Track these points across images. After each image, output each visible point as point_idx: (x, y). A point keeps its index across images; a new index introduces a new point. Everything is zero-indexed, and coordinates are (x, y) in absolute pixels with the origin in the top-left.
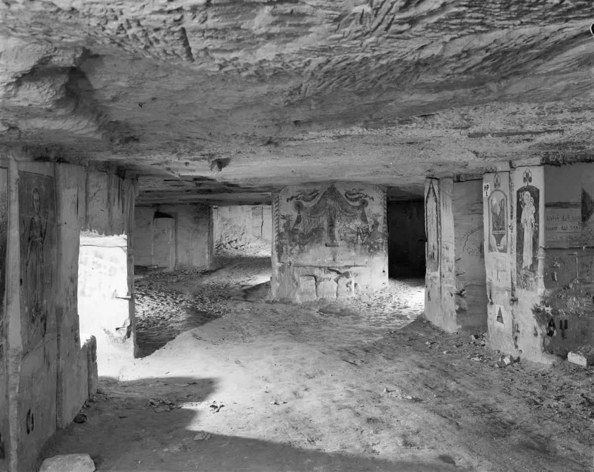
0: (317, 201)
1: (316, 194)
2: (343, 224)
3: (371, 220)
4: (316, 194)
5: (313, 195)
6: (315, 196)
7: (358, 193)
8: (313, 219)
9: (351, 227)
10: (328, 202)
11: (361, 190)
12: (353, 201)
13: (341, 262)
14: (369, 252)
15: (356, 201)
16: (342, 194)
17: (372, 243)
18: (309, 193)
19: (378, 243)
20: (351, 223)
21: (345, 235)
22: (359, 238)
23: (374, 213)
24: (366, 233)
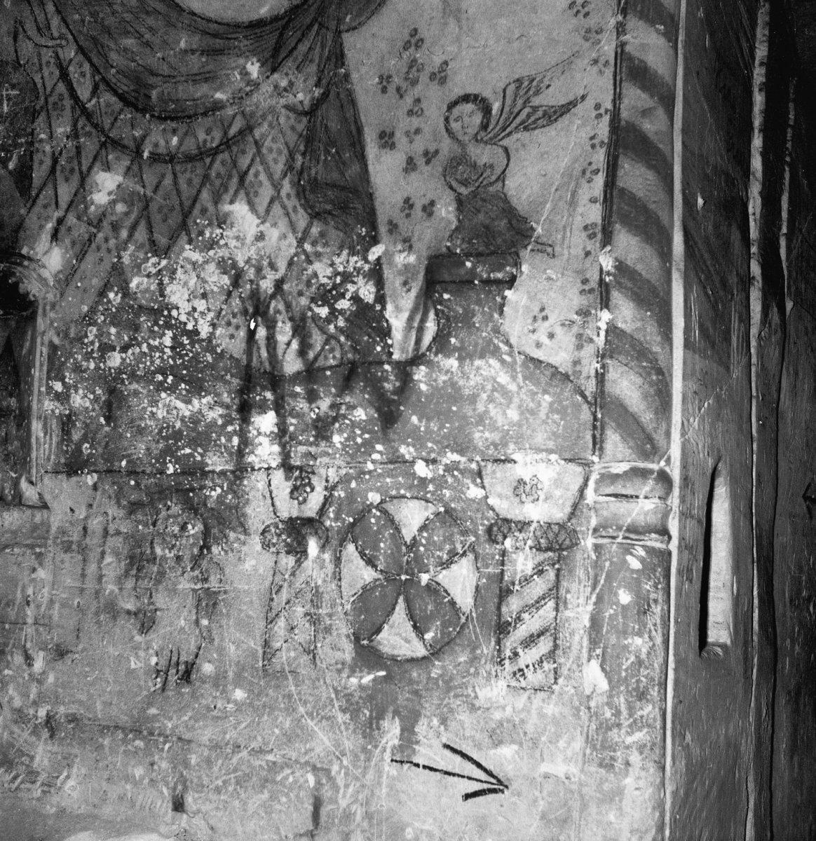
2: (93, 272)
3: (426, 185)
9: (177, 294)
13: (42, 754)
14: (368, 655)
17: (412, 516)
19: (500, 528)
21: (113, 403)
22: (266, 452)
23: (461, 83)
24: (349, 376)
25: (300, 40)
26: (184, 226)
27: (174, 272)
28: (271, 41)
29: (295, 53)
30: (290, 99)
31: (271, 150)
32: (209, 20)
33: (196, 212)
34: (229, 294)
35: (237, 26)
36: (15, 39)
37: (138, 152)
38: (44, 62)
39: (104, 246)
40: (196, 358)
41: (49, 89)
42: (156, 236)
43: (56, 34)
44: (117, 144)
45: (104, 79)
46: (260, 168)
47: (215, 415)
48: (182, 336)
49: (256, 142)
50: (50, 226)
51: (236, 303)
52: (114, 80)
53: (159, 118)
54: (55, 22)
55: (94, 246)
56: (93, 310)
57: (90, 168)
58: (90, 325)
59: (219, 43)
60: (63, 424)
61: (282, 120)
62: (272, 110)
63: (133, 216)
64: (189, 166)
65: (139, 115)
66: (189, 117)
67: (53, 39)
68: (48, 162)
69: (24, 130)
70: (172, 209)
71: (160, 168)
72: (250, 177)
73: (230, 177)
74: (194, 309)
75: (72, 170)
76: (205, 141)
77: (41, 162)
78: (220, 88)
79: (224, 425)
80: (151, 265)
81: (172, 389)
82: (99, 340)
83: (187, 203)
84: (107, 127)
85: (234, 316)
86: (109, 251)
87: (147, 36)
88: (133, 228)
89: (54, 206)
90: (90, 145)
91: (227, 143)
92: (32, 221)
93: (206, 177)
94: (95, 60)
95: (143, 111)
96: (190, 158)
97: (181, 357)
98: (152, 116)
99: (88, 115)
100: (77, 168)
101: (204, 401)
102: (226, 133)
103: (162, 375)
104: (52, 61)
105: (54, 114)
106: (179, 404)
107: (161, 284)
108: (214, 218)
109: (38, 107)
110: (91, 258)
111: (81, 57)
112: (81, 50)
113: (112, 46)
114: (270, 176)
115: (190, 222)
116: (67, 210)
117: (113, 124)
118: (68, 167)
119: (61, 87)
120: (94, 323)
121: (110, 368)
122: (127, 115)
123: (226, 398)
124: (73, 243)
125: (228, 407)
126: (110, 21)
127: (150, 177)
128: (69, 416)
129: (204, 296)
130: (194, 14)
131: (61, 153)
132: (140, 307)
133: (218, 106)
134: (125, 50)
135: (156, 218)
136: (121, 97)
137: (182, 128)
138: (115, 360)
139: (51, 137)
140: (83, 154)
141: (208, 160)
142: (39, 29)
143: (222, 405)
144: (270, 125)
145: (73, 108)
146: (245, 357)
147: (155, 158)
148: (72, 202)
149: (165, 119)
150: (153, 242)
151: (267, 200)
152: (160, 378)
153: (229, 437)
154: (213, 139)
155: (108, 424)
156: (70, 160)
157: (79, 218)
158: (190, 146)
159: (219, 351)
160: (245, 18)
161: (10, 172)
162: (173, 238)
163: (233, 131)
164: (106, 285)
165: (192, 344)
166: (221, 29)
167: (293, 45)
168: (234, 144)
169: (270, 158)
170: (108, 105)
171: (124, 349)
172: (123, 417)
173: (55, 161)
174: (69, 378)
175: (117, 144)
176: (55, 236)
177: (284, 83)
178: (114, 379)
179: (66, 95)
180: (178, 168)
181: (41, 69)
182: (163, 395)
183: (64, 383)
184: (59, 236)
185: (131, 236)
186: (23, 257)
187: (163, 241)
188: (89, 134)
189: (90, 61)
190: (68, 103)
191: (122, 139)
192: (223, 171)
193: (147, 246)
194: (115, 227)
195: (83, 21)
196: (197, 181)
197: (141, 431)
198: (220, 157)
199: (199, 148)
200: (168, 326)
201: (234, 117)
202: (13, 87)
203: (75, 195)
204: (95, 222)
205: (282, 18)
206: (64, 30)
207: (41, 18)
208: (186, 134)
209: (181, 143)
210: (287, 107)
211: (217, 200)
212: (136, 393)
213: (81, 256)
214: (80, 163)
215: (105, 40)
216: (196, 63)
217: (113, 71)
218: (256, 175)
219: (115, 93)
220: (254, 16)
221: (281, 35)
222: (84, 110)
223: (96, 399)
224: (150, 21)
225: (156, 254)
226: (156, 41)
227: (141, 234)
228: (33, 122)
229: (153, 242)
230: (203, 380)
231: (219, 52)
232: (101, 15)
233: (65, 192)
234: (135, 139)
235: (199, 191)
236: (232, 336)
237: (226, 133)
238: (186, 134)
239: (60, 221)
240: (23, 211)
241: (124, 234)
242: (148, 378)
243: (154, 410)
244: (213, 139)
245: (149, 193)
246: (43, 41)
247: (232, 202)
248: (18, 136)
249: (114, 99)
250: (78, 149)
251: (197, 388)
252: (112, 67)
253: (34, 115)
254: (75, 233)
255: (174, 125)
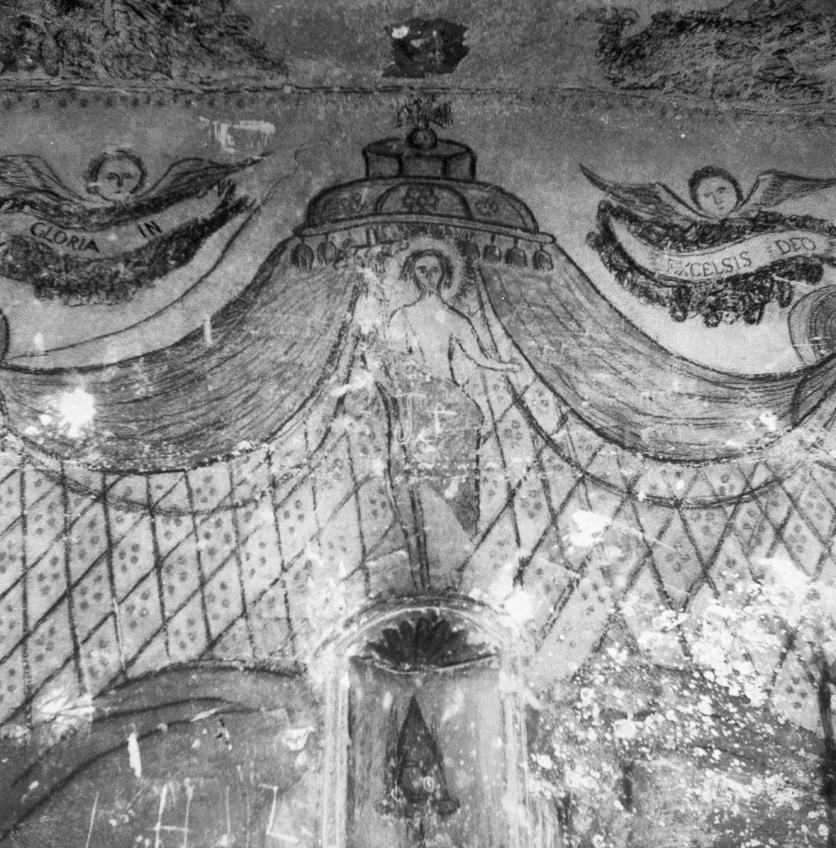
0: (216, 296)
1: (202, 208)
4: (202, 208)
5: (170, 220)
6: (191, 237)
7: (764, 223)
8: (130, 527)
9: (708, 653)
10: (367, 316)
11: (812, 185)
12: (713, 314)
15: (752, 315)
16: (550, 221)
18: (110, 193)
20: (707, 605)
25: (822, 400)
26: (705, 576)
27: (699, 628)
28: (788, 396)
29: (819, 411)
30: (821, 455)
31: (811, 505)
32: (705, 368)
33: (720, 561)
34: (783, 657)
35: (741, 377)
36: (450, 356)
37: (630, 492)
38: (490, 383)
39: (593, 595)
40: (749, 728)
41: (497, 416)
42: (667, 587)
43: (506, 358)
44: (598, 481)
45: (573, 411)
46: (802, 523)
47: (788, 797)
48: (726, 702)
49: (789, 495)
50: (510, 567)
51: (794, 667)
52: (586, 414)
53: (655, 458)
54: (505, 345)
55: (577, 592)
56: (586, 669)
57: (564, 505)
58: (584, 685)
59: (721, 391)
60: (559, 810)
61: (817, 475)
62: (802, 464)
63: (631, 564)
64: (704, 513)
65: (627, 454)
66: (697, 462)
67: (501, 362)
68: (501, 495)
69: (466, 455)
70: (687, 558)
71: (662, 513)
72: (789, 531)
73: (762, 529)
74: (737, 672)
75: (538, 506)
76: (722, 489)
77: (492, 494)
78: (732, 434)
79: (804, 811)
80: (666, 617)
81: (721, 766)
82: (600, 705)
83: (706, 554)
84: (583, 463)
85: (796, 681)
86: (601, 600)
87: (627, 374)
88: (635, 575)
89: (514, 544)
90: (562, 480)
91: (751, 493)
92: (482, 559)
93: (729, 527)
94: (560, 390)
95: (633, 449)
96: (703, 505)
97: (729, 727)
98: (646, 456)
99: (557, 448)
100: (545, 503)
101: (770, 781)
102: (748, 483)
103: (705, 748)
104: (502, 385)
105: (506, 443)
106: (732, 784)
107: (683, 641)
108: (747, 571)
109: (483, 433)
110: (575, 606)
111: (541, 386)
112: (541, 378)
113: (581, 377)
114: (816, 532)
115: (713, 574)
116: (535, 550)
117: (591, 460)
118: (532, 501)
119: (515, 414)
120: (591, 684)
121: (621, 740)
122: (611, 451)
123: (801, 776)
124: (548, 589)
125: (806, 788)
126: (576, 353)
127: (652, 520)
128: (566, 801)
129: (747, 657)
130: (684, 359)
131: (519, 485)
132: (658, 667)
133: (731, 455)
134: (598, 384)
135: (666, 568)
136: (600, 432)
137: (689, 472)
138: (626, 730)
139: (504, 465)
140: (552, 487)
141: (730, 509)
142: (482, 350)
143: (797, 786)
144: (803, 479)
145: (533, 438)
146: (821, 729)
147: (655, 501)
148: (541, 541)
149: (664, 460)
150: (665, 594)
151: (816, 557)
152: (701, 752)
153: (814, 826)
154: (732, 487)
155: (628, 809)
156: (534, 494)
157: (552, 560)
158: (702, 491)
159: (782, 721)
160: (750, 369)
161: (447, 501)
162: (692, 589)
163: (756, 482)
164: (602, 639)
165: (742, 711)
166: (723, 378)
167: (815, 403)
168: (761, 494)
169: (811, 513)
170: (582, 439)
171: (641, 716)
172: (649, 800)
173: (512, 494)
174: (561, 751)
175: (598, 481)
176: (519, 577)
177: (811, 439)
178: (629, 753)
179: (523, 422)
180: (688, 514)
181: (486, 391)
182: (709, 773)
183: (553, 757)
184: (525, 578)
185: (631, 585)
186: (472, 601)
187: (679, 593)
188: (560, 468)
189: (552, 389)
190: (526, 431)
191: (605, 476)
192: (752, 522)
193: (657, 598)
194: (607, 573)
195: (541, 349)
196: (717, 530)
197: (680, 819)
198: (744, 508)
199: (714, 495)
200: (702, 689)
201: (756, 466)
202: (449, 406)
203: (545, 533)
204: (576, 566)
205: (795, 376)
206: (516, 355)
207: (486, 340)
208: (695, 478)
209: (689, 488)
210: (819, 463)
211: (748, 550)
212: (666, 771)
213: (562, 603)
214: (548, 499)
215: (572, 371)
216: (696, 408)
217: (585, 404)
218: (797, 529)
219: (591, 427)
220: (761, 371)
221: (797, 392)
222: (549, 441)
223: (605, 779)
224: (628, 359)
225: (670, 605)
226: (638, 379)
227: (646, 582)
228: (478, 448)
229: (665, 594)
230: (765, 756)
231: (726, 400)
232: (564, 346)
233: (531, 529)
234: (624, 478)
235: (721, 541)
236: (797, 705)
237: (748, 483)
238: (695, 478)
239: (525, 563)
240: (468, 547)
241: (621, 581)
242: (683, 751)
243: (698, 791)
244: (732, 487)
245: (651, 538)
246: (488, 363)
247: (769, 555)
248: (454, 461)
249: (590, 434)
250: (546, 485)
251: (758, 764)
252: (583, 399)
253: (479, 441)
254: (547, 575)
255: (677, 467)
